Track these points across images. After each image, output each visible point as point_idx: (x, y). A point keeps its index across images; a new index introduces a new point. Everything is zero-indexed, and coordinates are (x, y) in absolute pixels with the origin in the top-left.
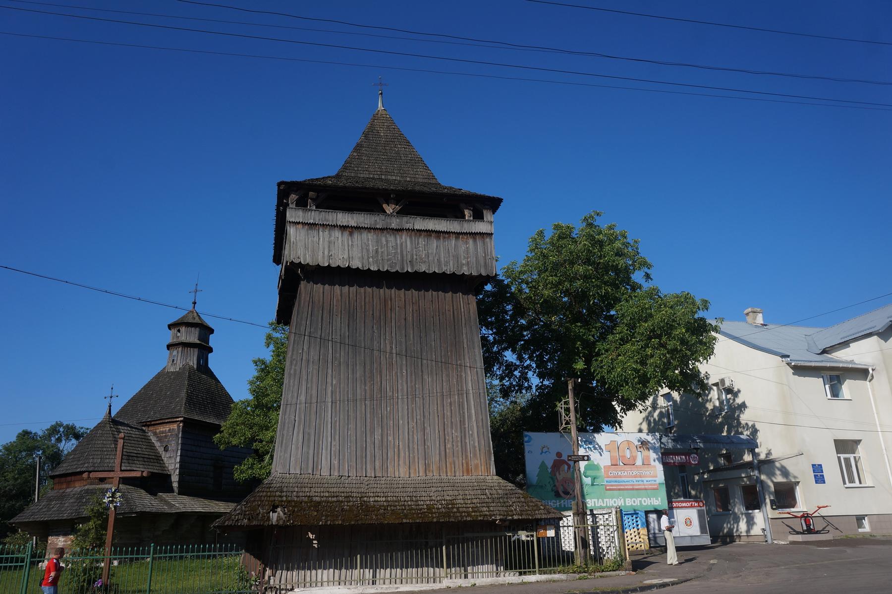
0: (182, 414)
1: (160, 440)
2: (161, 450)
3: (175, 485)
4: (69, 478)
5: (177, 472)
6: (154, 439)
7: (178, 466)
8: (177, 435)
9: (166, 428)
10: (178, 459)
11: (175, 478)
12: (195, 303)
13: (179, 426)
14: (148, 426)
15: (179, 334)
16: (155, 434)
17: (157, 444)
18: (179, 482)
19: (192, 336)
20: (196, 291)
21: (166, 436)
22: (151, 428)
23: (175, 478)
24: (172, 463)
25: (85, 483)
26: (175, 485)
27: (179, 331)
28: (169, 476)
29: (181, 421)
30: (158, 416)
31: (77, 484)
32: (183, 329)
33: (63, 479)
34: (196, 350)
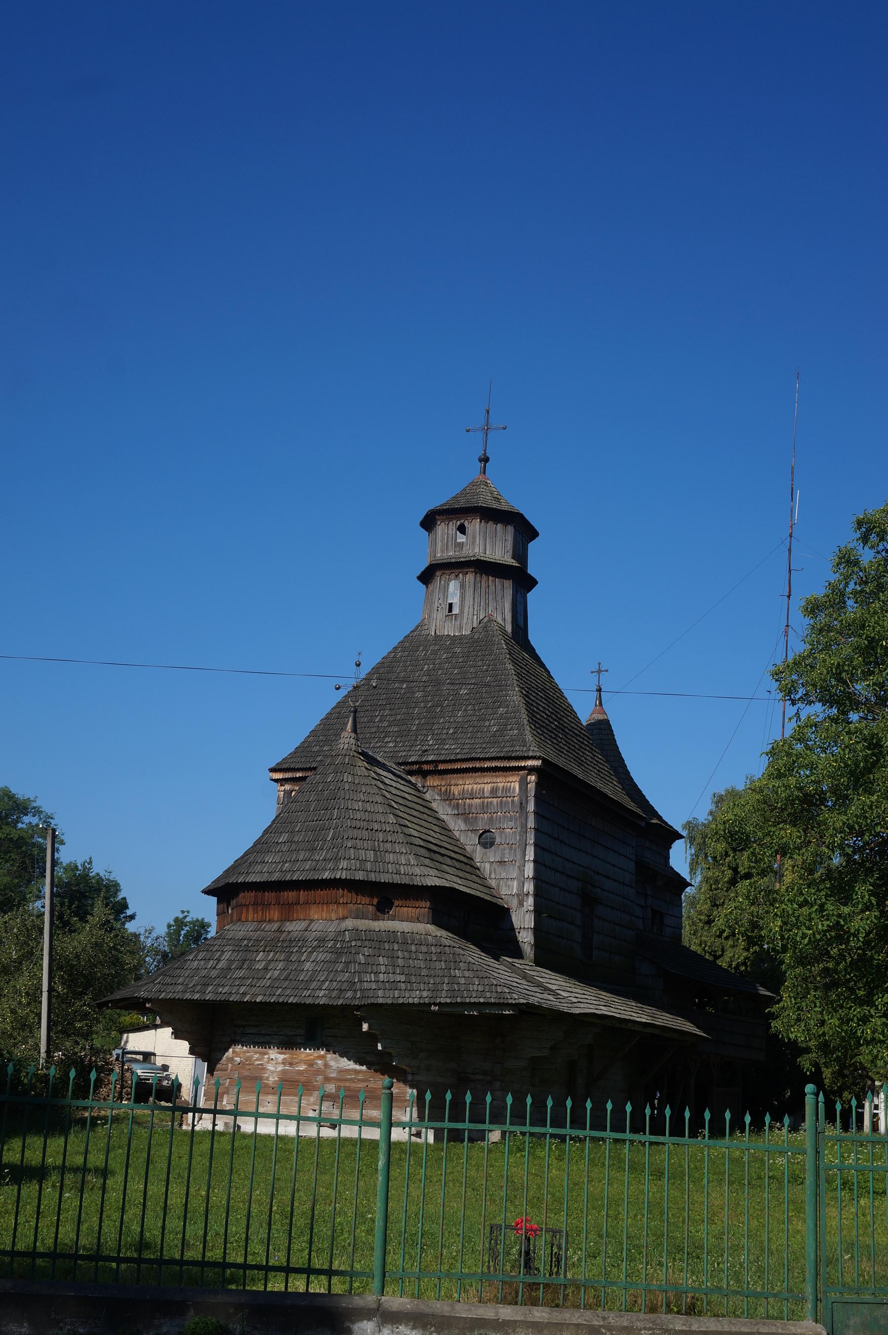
0: (534, 750)
1: (464, 815)
2: (469, 842)
3: (526, 938)
4: (290, 895)
5: (530, 902)
6: (444, 811)
7: (529, 887)
8: (522, 806)
9: (484, 784)
10: (529, 870)
11: (523, 921)
12: (485, 460)
13: (524, 783)
14: (424, 774)
15: (461, 539)
16: (448, 797)
17: (457, 826)
18: (537, 931)
19: (492, 544)
20: (487, 430)
21: (484, 808)
22: (431, 781)
23: (523, 921)
24: (512, 880)
25: (341, 911)
26: (526, 938)
27: (462, 529)
28: (505, 912)
29: (531, 770)
30: (451, 749)
31: (315, 913)
32: (475, 525)
33: (269, 896)
34: (508, 584)
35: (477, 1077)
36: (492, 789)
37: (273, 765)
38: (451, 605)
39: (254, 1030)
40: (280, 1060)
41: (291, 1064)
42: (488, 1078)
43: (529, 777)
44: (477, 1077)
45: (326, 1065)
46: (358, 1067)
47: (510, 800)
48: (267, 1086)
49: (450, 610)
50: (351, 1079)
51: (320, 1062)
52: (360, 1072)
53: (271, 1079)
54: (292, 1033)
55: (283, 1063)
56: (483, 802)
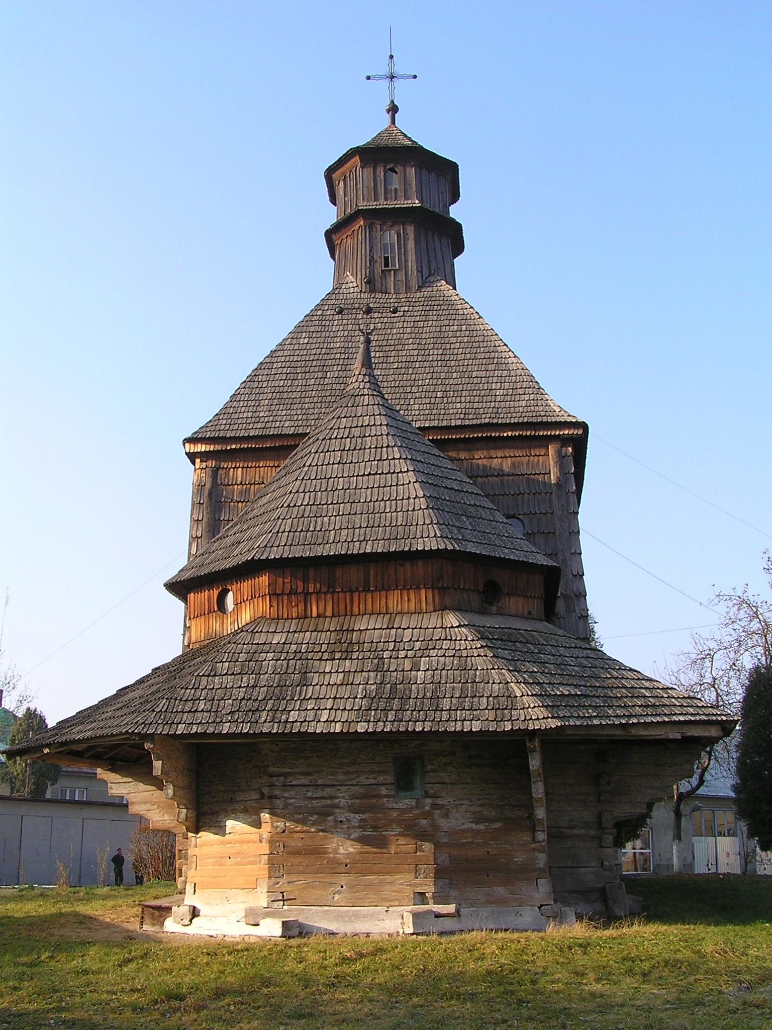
12: (393, 109)
35: (576, 831)
36: (513, 464)
37: (188, 435)
38: (386, 259)
39: (304, 780)
40: (355, 823)
41: (375, 828)
42: (593, 832)
43: (564, 449)
44: (576, 831)
45: (435, 826)
46: (474, 826)
47: (540, 478)
48: (335, 862)
49: (387, 265)
50: (468, 844)
51: (424, 822)
52: (478, 832)
53: (341, 850)
54: (372, 781)
55: (359, 827)
56: (502, 482)
